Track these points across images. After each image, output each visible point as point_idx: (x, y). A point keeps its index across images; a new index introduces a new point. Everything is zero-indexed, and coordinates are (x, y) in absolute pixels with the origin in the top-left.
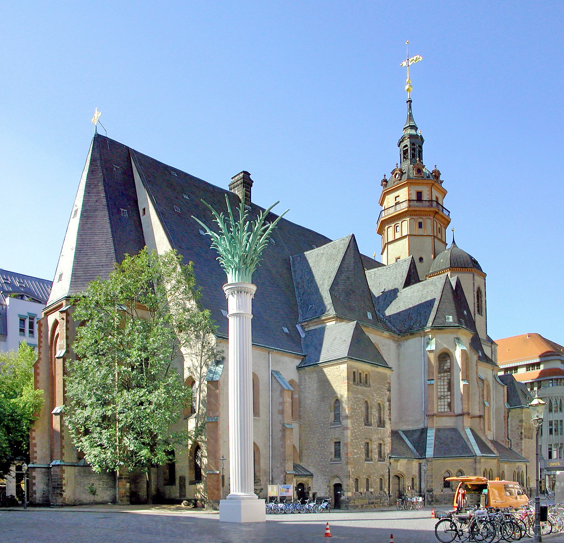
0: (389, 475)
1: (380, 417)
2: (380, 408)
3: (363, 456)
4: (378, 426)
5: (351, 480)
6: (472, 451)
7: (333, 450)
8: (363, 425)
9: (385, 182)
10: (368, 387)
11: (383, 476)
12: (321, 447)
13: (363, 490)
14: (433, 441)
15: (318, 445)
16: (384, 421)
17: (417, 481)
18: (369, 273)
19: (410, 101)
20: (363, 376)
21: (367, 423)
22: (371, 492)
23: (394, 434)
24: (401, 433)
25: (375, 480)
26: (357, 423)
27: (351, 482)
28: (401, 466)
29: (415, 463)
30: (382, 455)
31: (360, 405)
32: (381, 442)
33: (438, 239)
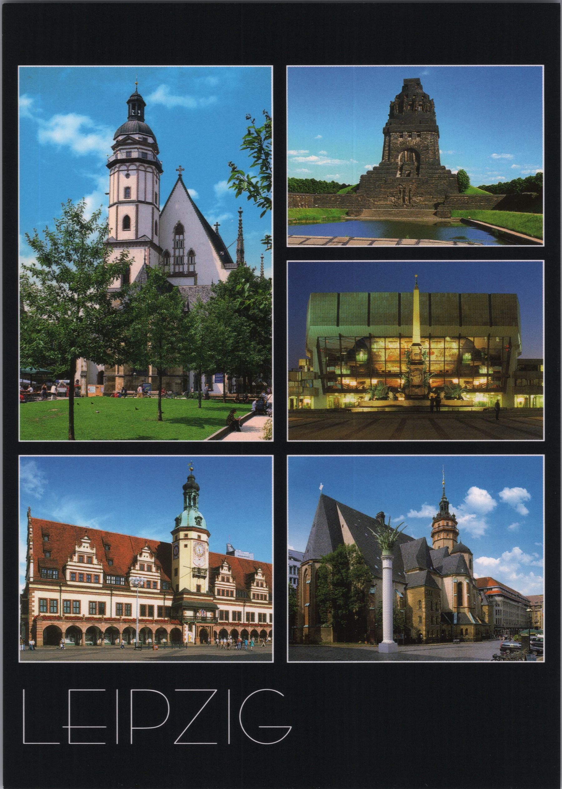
1: (436, 608)
2: (436, 605)
23: (441, 614)
28: (445, 627)
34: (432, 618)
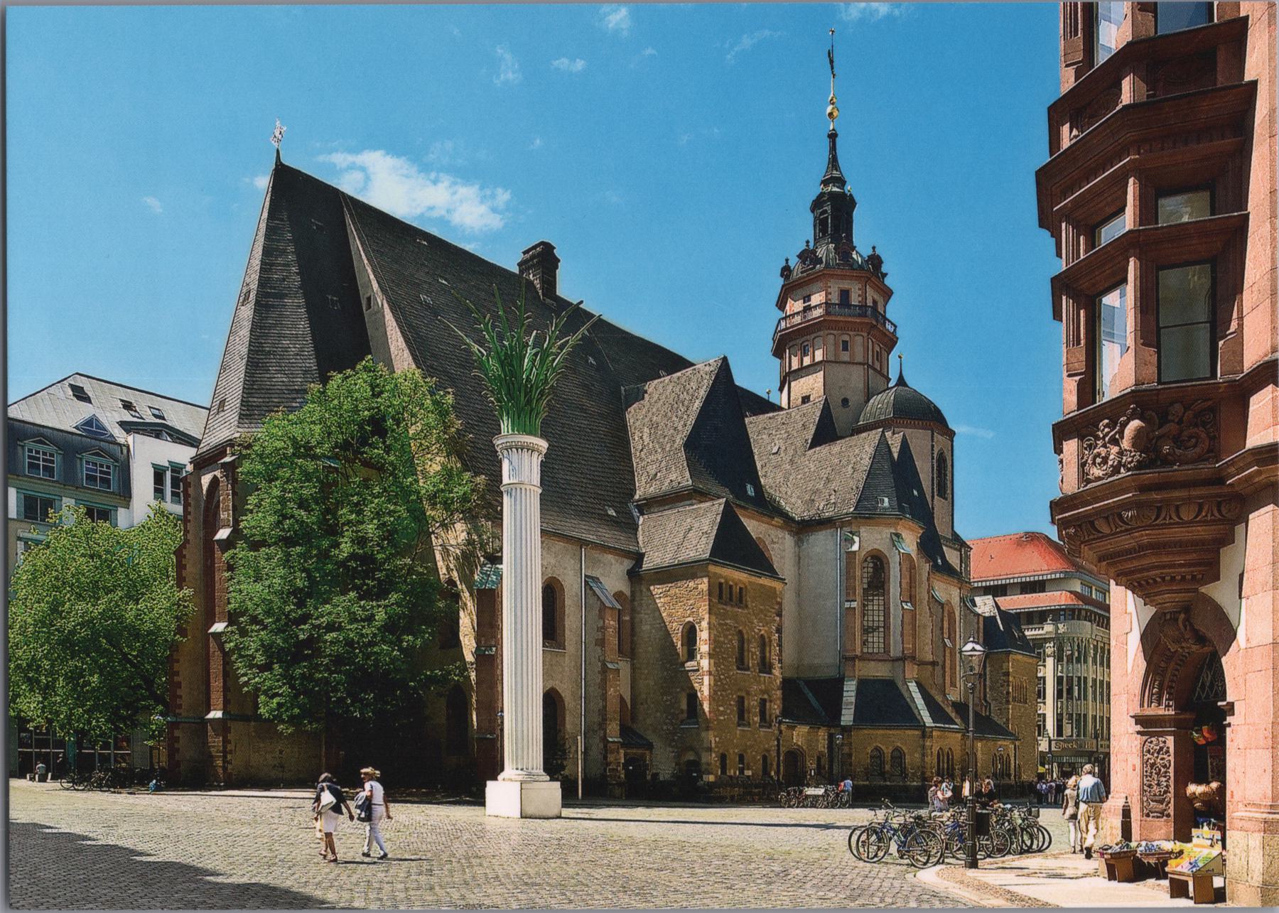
0: (778, 750)
1: (763, 658)
3: (736, 719)
4: (760, 672)
5: (714, 755)
6: (919, 717)
7: (684, 706)
9: (786, 271)
10: (743, 608)
11: (768, 751)
13: (735, 773)
14: (853, 700)
18: (754, 424)
19: (833, 136)
20: (736, 590)
21: (741, 664)
23: (788, 684)
24: (802, 684)
25: (754, 757)
28: (799, 735)
29: (822, 734)
30: (768, 717)
32: (766, 696)
33: (875, 369)
34: (741, 701)
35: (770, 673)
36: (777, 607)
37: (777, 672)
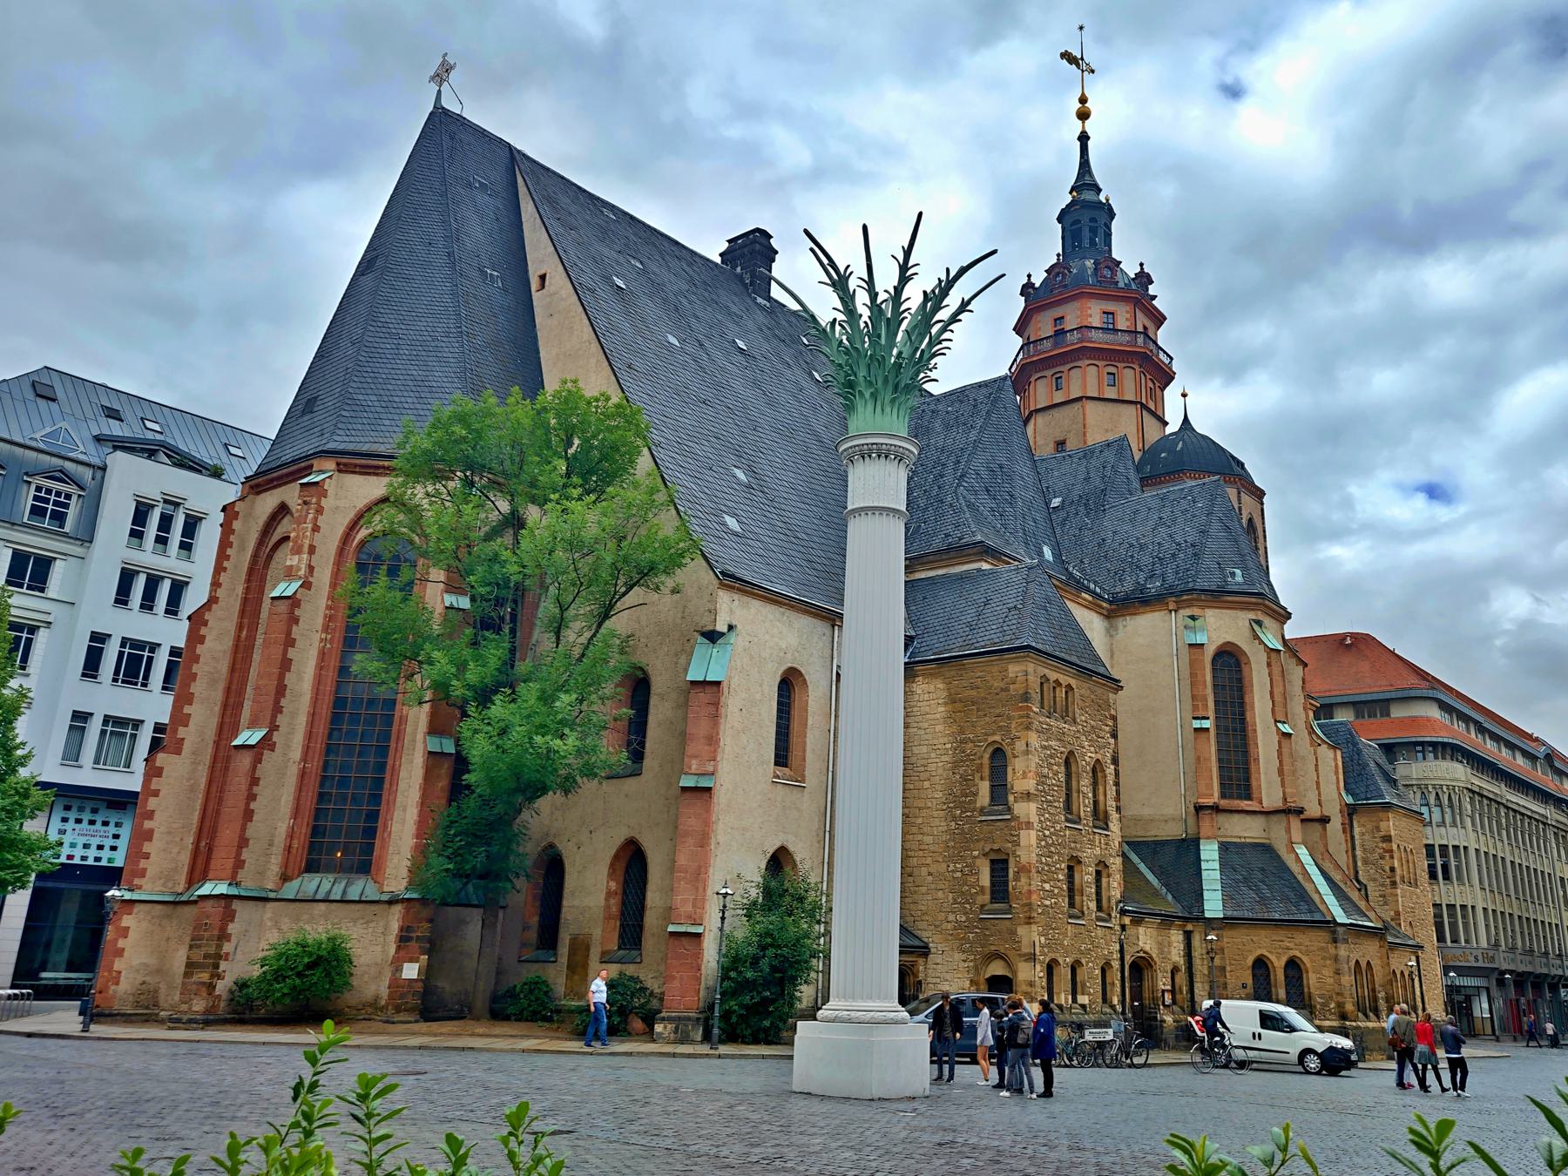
3: (1065, 903)
5: (1038, 967)
6: (1322, 907)
7: (985, 880)
8: (1063, 818)
12: (953, 871)
13: (1066, 999)
15: (944, 865)
16: (1106, 812)
17: (1181, 979)
22: (1083, 1006)
26: (1049, 813)
27: (1040, 972)
31: (1055, 768)
35: (1107, 829)
36: (1110, 723)
37: (1114, 826)
